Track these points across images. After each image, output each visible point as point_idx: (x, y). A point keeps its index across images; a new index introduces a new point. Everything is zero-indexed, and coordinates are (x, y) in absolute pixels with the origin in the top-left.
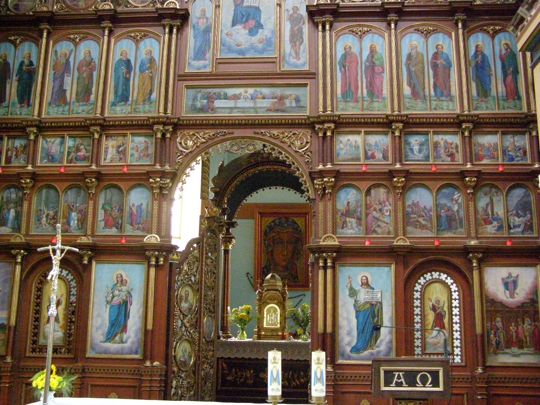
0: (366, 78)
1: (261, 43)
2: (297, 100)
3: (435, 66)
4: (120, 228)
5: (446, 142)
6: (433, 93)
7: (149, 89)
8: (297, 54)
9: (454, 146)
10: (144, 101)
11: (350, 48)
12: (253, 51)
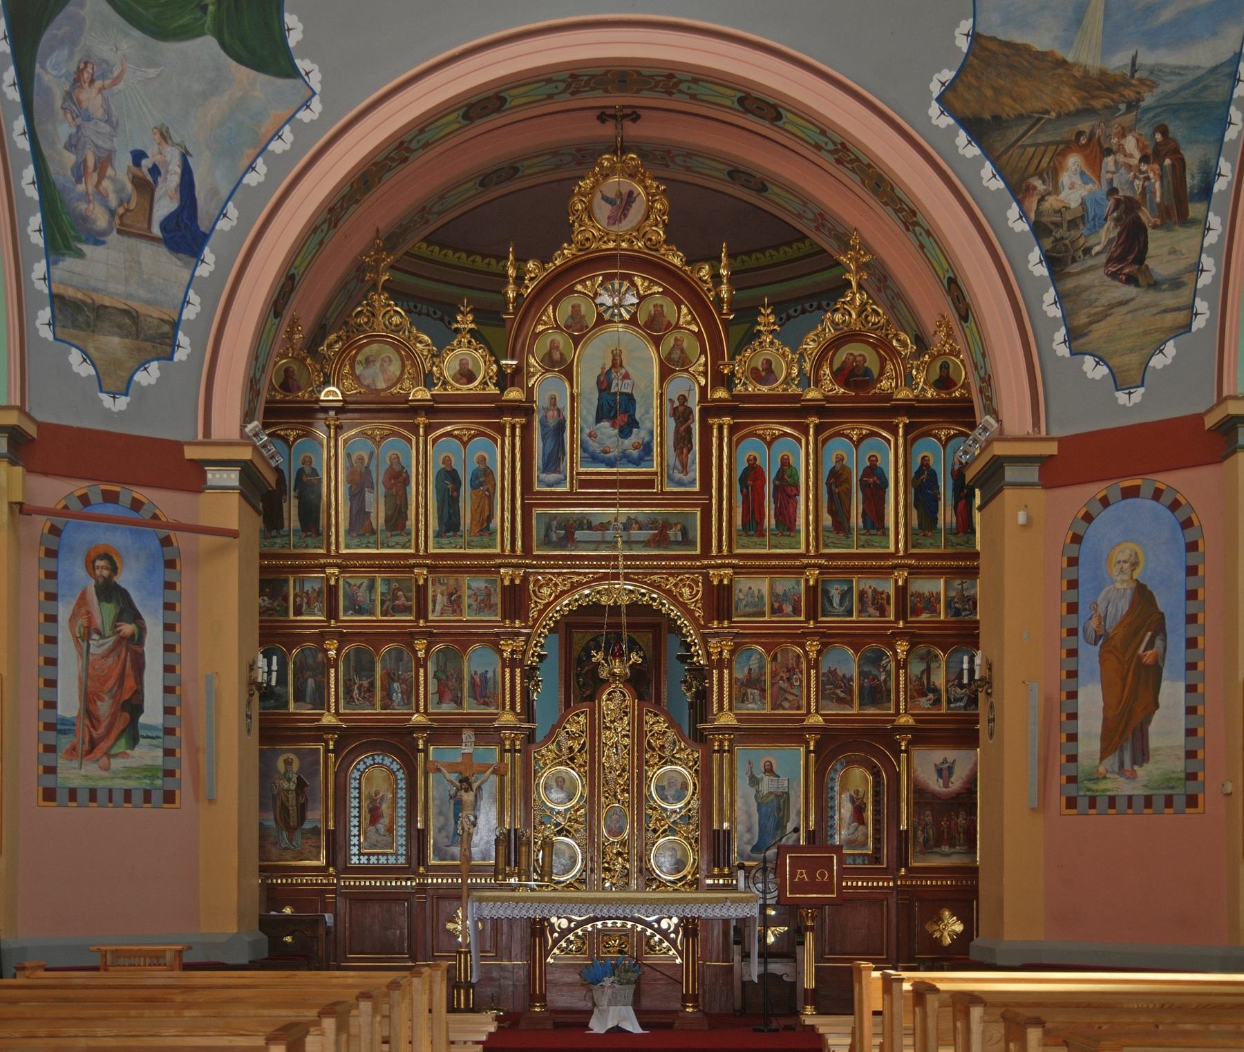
0: (775, 502)
1: (636, 448)
2: (684, 532)
3: (863, 484)
4: (458, 702)
5: (875, 591)
6: (861, 524)
7: (487, 514)
8: (684, 468)
9: (884, 596)
10: (481, 530)
11: (755, 459)
12: (625, 460)
